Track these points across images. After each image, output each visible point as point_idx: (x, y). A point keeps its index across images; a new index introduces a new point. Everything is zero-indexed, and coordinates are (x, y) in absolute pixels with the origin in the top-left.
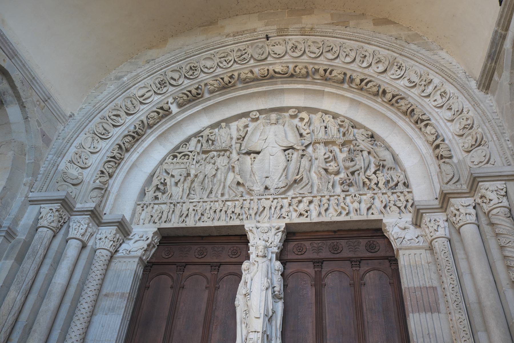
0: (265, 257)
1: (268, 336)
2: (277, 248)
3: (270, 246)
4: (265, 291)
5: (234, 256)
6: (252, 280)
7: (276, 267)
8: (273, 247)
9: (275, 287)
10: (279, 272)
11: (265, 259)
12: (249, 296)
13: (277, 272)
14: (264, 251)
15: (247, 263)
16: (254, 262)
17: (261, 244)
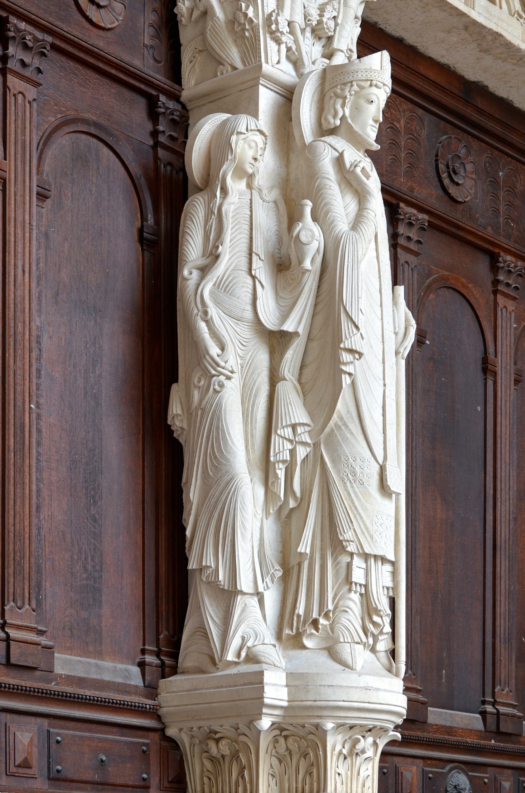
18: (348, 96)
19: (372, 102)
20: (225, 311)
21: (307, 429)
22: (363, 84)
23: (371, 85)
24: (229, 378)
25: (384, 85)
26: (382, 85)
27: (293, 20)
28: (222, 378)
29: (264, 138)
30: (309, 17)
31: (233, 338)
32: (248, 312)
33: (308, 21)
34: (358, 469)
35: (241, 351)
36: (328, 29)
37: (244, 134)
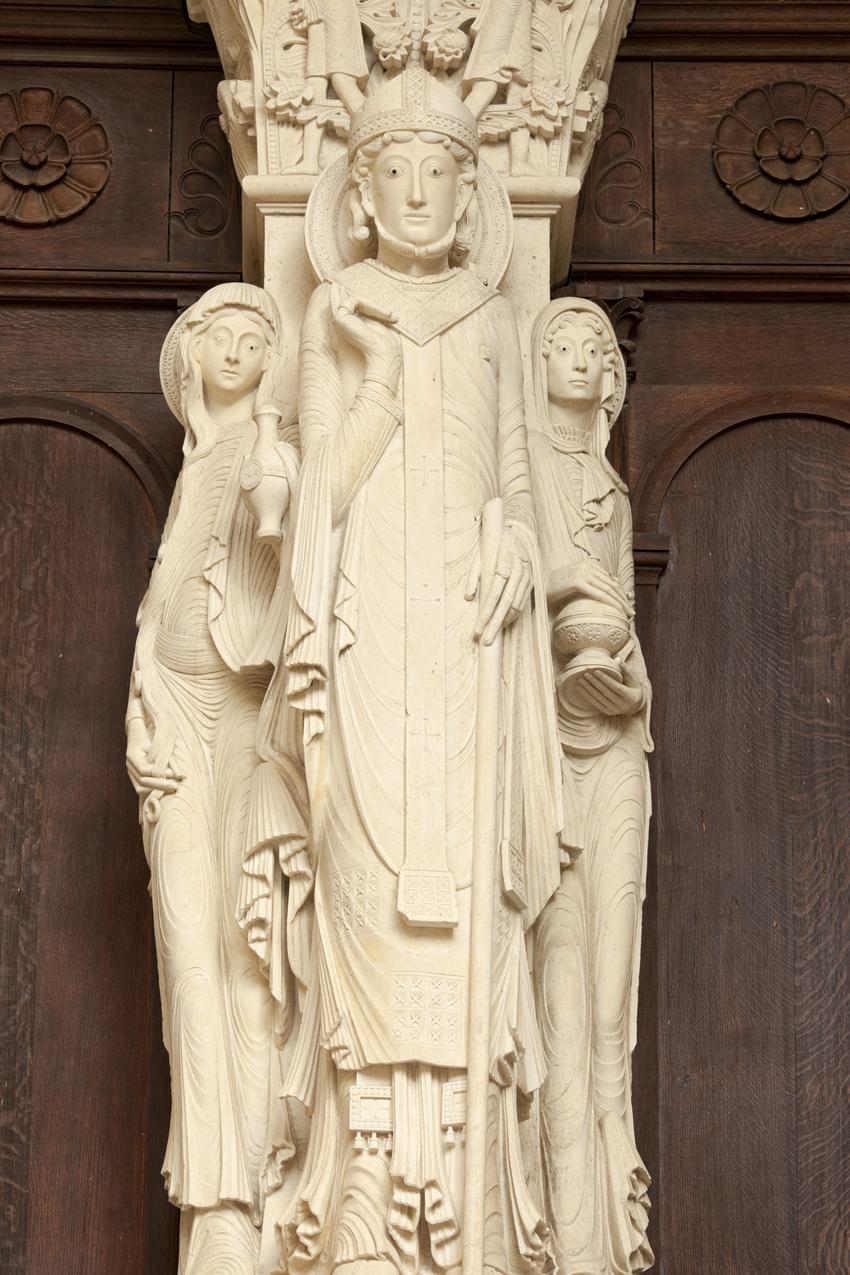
0: (455, 257)
1: (523, 1101)
2: (562, 147)
3: (493, 128)
4: (492, 653)
5: (34, 209)
6: (340, 520)
7: (565, 365)
8: (520, 139)
9: (577, 595)
10: (590, 425)
11: (457, 290)
12: (318, 701)
13: (563, 419)
14: (452, 195)
15: (239, 321)
16: (355, 325)
17: (419, 119)
18: (359, 180)
19: (394, 172)
20: (170, 665)
21: (297, 845)
22: (368, 147)
23: (386, 144)
24: (169, 792)
25: (416, 131)
26: (412, 133)
27: (332, 71)
28: (155, 795)
29: (254, 315)
30: (384, 50)
31: (187, 711)
32: (206, 653)
33: (385, 57)
34: (353, 897)
35: (209, 731)
36: (441, 51)
37: (200, 322)
